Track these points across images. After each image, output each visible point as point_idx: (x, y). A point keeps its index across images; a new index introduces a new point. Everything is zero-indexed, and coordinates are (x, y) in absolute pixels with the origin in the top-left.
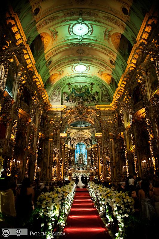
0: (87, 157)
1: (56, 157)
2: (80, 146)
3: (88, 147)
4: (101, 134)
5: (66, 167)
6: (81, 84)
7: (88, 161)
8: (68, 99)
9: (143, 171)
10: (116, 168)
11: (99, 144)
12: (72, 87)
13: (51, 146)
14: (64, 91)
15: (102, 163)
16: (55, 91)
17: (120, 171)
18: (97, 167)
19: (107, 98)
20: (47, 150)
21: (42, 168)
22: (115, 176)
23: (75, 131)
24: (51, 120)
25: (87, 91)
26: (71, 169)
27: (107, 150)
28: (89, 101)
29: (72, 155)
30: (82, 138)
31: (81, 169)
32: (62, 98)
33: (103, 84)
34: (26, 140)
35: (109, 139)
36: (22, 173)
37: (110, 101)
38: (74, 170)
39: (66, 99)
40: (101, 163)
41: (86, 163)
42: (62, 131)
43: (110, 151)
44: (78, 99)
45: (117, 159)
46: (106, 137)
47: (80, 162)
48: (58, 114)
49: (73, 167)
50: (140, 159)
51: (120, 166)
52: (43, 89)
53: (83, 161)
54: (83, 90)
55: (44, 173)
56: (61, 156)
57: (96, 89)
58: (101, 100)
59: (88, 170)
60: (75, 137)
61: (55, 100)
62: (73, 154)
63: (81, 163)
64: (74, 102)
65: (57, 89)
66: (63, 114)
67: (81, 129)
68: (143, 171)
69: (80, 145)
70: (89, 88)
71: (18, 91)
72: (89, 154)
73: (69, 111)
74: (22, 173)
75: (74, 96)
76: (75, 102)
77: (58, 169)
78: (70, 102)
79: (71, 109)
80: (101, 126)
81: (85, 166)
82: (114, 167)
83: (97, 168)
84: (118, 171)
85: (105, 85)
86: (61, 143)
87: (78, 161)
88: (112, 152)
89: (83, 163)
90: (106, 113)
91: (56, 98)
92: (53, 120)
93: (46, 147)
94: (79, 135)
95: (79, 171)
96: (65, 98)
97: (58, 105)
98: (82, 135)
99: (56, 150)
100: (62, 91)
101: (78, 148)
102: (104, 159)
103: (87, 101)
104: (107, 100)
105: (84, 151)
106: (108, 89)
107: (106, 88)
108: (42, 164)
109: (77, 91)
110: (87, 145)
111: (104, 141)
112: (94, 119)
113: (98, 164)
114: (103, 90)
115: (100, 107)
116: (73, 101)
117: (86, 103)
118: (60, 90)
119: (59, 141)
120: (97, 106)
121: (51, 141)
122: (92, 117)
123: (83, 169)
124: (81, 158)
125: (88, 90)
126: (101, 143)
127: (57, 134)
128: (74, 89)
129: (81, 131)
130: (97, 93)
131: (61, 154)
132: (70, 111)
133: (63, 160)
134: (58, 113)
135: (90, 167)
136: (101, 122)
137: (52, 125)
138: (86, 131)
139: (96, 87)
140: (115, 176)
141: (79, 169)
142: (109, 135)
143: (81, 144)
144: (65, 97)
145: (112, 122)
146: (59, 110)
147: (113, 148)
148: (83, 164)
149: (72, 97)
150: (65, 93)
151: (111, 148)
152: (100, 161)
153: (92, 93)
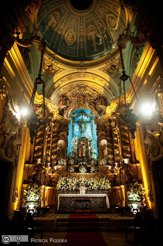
0: (99, 141)
2: (81, 127)
3: (99, 118)
5: (38, 157)
7: (101, 149)
23: (68, 70)
26: (55, 168)
29: (62, 133)
30: (84, 97)
31: (83, 171)
38: (65, 172)
41: (95, 157)
47: (80, 152)
49: (63, 162)
53: (87, 152)
59: (101, 173)
60: (69, 94)
62: (62, 131)
63: (84, 155)
67: (82, 66)
69: (80, 123)
72: (103, 131)
81: (93, 162)
87: (75, 153)
89: (87, 156)
95: (78, 174)
98: (84, 87)
101: (76, 128)
105: (90, 132)
110: (96, 112)
123: (88, 170)
124: (82, 143)
135: (108, 164)
138: (95, 70)
141: (77, 170)
143: (84, 123)
148: (89, 160)
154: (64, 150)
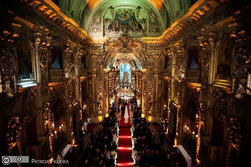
0: (131, 78)
1: (100, 92)
4: (146, 69)
5: (112, 89)
6: (126, 7)
8: (110, 27)
9: (184, 133)
10: (158, 104)
11: (143, 80)
12: (115, 12)
13: (95, 81)
14: (106, 17)
15: (145, 98)
16: (95, 17)
17: (161, 105)
18: (140, 90)
19: (155, 28)
20: (91, 86)
21: (88, 104)
22: (156, 111)
24: (93, 55)
25: (133, 18)
27: (151, 86)
28: (134, 31)
29: (117, 76)
30: (126, 59)
31: (125, 88)
32: (104, 27)
33: (152, 9)
34: (65, 102)
35: (154, 75)
36: (67, 133)
37: (158, 31)
39: (108, 28)
40: (144, 97)
41: (130, 82)
42: (105, 66)
43: (154, 88)
44: (122, 28)
45: (160, 95)
46: (151, 74)
47: (124, 81)
48: (100, 46)
50: (183, 121)
51: (161, 102)
52: (79, 29)
53: (127, 79)
54: (128, 16)
55: (90, 107)
56: (105, 91)
57: (143, 15)
58: (148, 30)
60: (120, 59)
61: (95, 30)
64: (117, 31)
65: (97, 15)
66: (106, 47)
68: (184, 133)
70: (135, 12)
71: (42, 65)
72: (133, 75)
73: (112, 44)
74: (67, 133)
75: (117, 24)
76: (119, 31)
77: (103, 104)
78: (113, 32)
79: (114, 41)
80: (146, 60)
82: (156, 102)
83: (140, 91)
84: (159, 106)
85: (155, 11)
86: (104, 78)
88: (155, 88)
89: (127, 81)
90: (154, 47)
91: (97, 27)
92: (94, 55)
93: (90, 83)
94: (123, 57)
96: (108, 27)
97: (99, 37)
99: (100, 87)
100: (104, 17)
102: (147, 95)
103: (133, 31)
104: (154, 30)
106: (158, 16)
107: (155, 14)
108: (88, 101)
109: (121, 17)
111: (148, 77)
112: (140, 53)
113: (141, 98)
114: (151, 17)
115: (147, 40)
116: (116, 30)
117: (130, 33)
118: (101, 17)
119: (102, 76)
120: (143, 38)
121: (94, 77)
122: (137, 51)
123: (127, 88)
125: (134, 16)
126: (146, 79)
127: (100, 69)
128: (117, 15)
129: (125, 55)
130: (144, 20)
131: (106, 90)
132: (113, 43)
133: (108, 95)
134: (100, 45)
136: (147, 57)
137: (95, 60)
139: (144, 12)
140: (156, 110)
141: (123, 88)
142: (154, 71)
144: (107, 26)
145: (158, 57)
146: (100, 43)
147: (157, 84)
148: (128, 83)
149: (115, 25)
150: (107, 20)
151: (155, 85)
152: (143, 96)
153: (138, 21)
154: (119, 81)
